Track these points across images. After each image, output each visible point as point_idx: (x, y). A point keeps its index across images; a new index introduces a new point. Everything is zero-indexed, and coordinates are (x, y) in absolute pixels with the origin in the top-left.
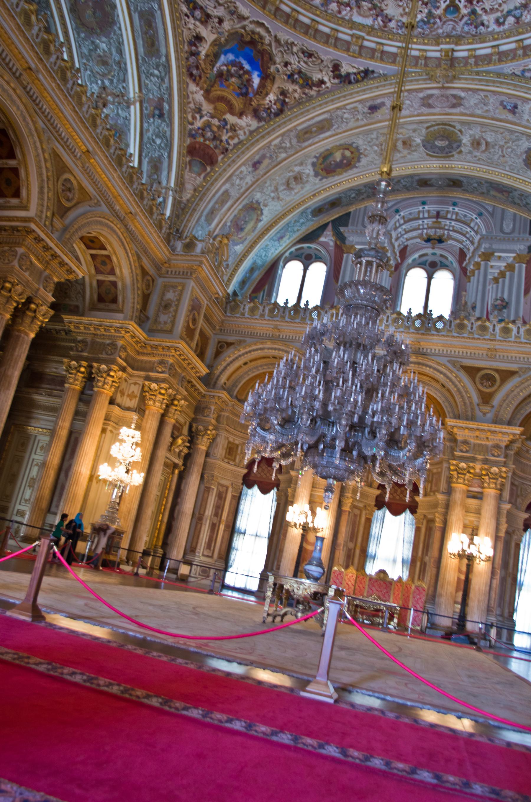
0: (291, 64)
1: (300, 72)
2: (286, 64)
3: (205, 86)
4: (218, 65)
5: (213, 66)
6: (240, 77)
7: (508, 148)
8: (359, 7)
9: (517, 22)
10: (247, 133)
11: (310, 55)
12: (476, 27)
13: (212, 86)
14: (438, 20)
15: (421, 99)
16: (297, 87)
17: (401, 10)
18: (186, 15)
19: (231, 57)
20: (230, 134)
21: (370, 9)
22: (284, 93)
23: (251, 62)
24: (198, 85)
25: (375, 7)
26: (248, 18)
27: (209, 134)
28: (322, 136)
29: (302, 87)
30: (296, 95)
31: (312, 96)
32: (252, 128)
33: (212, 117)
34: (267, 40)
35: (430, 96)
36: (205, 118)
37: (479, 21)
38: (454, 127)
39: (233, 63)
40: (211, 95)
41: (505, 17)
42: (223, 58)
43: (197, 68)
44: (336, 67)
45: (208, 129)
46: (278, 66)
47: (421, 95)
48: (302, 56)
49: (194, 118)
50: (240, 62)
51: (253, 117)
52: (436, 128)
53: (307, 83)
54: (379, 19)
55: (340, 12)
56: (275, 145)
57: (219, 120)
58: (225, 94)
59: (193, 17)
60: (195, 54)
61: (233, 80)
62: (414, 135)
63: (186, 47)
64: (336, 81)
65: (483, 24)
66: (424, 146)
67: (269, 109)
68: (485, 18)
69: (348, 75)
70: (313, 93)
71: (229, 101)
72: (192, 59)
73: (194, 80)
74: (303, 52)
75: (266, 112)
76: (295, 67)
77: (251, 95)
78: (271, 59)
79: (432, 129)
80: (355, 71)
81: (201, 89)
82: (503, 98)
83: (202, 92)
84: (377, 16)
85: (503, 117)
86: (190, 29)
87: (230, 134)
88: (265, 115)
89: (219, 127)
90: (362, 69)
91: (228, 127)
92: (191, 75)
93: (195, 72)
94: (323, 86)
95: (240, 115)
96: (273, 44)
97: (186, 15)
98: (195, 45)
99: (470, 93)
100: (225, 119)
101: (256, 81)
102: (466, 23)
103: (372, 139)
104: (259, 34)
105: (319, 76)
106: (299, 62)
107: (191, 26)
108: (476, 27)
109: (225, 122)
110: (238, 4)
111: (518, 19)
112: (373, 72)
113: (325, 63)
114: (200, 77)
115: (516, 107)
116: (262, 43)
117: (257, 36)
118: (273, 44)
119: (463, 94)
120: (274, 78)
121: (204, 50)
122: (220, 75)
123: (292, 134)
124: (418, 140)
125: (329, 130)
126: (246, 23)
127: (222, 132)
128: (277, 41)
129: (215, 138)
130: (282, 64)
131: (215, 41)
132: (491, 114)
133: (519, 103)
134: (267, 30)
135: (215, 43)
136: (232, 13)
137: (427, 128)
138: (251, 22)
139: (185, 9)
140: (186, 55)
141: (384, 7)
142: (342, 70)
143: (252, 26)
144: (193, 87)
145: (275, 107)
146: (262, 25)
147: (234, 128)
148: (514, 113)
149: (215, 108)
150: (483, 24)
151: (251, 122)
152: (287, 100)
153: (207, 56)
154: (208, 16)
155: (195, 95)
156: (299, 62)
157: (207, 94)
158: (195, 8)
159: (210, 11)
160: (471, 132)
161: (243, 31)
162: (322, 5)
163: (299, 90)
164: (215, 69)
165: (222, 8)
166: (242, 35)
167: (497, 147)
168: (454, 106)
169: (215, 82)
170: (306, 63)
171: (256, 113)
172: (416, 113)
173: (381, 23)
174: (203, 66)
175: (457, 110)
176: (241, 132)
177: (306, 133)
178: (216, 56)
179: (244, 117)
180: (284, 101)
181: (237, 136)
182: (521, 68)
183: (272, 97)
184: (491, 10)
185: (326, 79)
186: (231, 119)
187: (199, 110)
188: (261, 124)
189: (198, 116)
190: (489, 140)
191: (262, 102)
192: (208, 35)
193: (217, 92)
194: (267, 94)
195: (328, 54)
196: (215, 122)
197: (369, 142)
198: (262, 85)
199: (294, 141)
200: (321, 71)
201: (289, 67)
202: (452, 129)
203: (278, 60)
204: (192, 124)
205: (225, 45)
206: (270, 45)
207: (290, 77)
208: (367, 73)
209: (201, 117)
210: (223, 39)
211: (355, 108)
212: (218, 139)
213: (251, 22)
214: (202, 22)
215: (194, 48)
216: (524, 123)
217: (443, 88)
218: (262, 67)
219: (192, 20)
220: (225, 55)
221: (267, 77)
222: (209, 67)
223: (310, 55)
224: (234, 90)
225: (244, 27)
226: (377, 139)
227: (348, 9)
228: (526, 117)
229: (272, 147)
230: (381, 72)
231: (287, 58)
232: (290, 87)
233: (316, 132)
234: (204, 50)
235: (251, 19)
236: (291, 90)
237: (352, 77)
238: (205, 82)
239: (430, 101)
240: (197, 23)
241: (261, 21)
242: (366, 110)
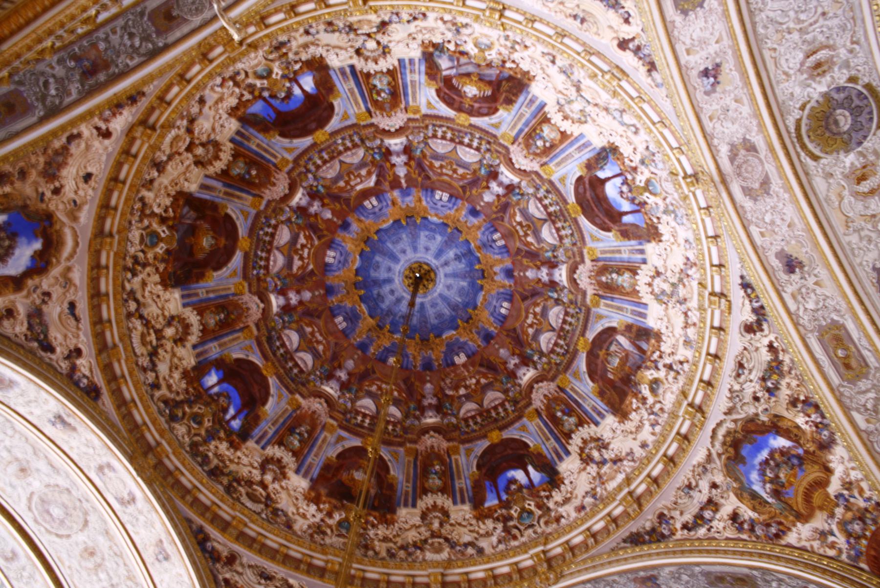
0: (755, 393)
1: (763, 379)
2: (756, 399)
3: (791, 518)
4: (764, 495)
5: (768, 503)
6: (778, 465)
7: (800, 21)
8: (685, 300)
9: (624, 111)
10: (853, 464)
11: (741, 365)
12: (653, 154)
13: (792, 508)
14: (668, 201)
15: (755, 200)
16: (784, 383)
17: (674, 247)
18: (709, 530)
19: (754, 476)
20: (856, 494)
21: (684, 285)
22: (794, 402)
23: (759, 449)
24: (789, 529)
25: (681, 280)
26: (709, 450)
27: (857, 527)
28: (855, 334)
29: (781, 375)
30: (794, 383)
31: (792, 361)
32: (846, 456)
33: (832, 515)
34: (730, 425)
35: (747, 191)
36: (834, 528)
37: (646, 153)
38: (798, 122)
39: (762, 473)
40: (803, 511)
41: (628, 126)
42: (757, 488)
43: (768, 525)
44: (749, 329)
45: (849, 527)
46: (760, 409)
47: (748, 204)
48: (743, 377)
49: (832, 546)
50: (760, 464)
51: (830, 453)
52: (810, 146)
53: (775, 368)
54: (690, 272)
55: (695, 324)
56: (868, 421)
57: (837, 505)
58: (801, 490)
59: (710, 521)
60: (753, 524)
61: (782, 475)
62: (838, 172)
63: (745, 536)
64: (765, 326)
65: (647, 148)
66: (860, 144)
67: (817, 427)
68: (641, 148)
69: (754, 311)
70: (786, 358)
71: (811, 485)
72: (759, 531)
73: (784, 533)
74: (739, 375)
75: (822, 430)
76: (758, 387)
77: (800, 451)
78: (752, 420)
79: (817, 152)
80: (747, 302)
81: (795, 525)
82: (699, 96)
83: (799, 525)
84: (688, 276)
85: (736, 74)
86: (724, 528)
87: (856, 494)
88: (826, 433)
89: (847, 508)
90: (742, 293)
91: (845, 492)
92: (777, 536)
93: (773, 530)
94: (775, 345)
95: (829, 471)
96: (735, 416)
97: (709, 530)
98: (742, 524)
99: (716, 142)
100: (836, 497)
101: (780, 442)
102: (656, 167)
103: (861, 239)
104: (724, 436)
105: (764, 351)
106: (751, 381)
107: (722, 524)
108: (653, 154)
109: (839, 496)
110: (695, 462)
111: (622, 111)
112: (742, 277)
113: (747, 345)
114: (780, 523)
115: (706, 73)
116: (735, 432)
117: (728, 439)
118: (735, 417)
119: (724, 151)
120: (776, 416)
121: (747, 513)
122: (776, 493)
123: (846, 392)
124: (850, 160)
125: (843, 327)
126: (713, 452)
127: (853, 504)
128: (729, 412)
129: (862, 519)
130: (757, 404)
131: (737, 495)
132: (742, 93)
133: (694, 73)
134: (719, 425)
135: (740, 497)
136: (705, 469)
137: (815, 158)
138: (713, 446)
139: (702, 531)
140: (754, 539)
141: (677, 270)
142: (751, 320)
143: (718, 445)
144: (791, 538)
145: (813, 416)
146: (714, 431)
147: (848, 485)
148: (718, 66)
149: (821, 508)
150: (647, 148)
151: (838, 457)
152: (802, 398)
153: (754, 509)
154: (710, 501)
155: (803, 536)
156: (751, 381)
157: (803, 518)
158: (702, 518)
159: (704, 498)
160: (797, 90)
161: (723, 457)
162: (692, 347)
163: (787, 380)
164: (770, 500)
165: (701, 483)
166: (728, 458)
167: (809, 37)
168: (752, 148)
169: (786, 503)
170: (751, 371)
171: (826, 446)
172: (786, 196)
173: (694, 269)
174: (765, 517)
175: (758, 141)
176: (855, 475)
177: (848, 366)
178: (754, 496)
179: (831, 465)
180: (804, 402)
181: (857, 481)
182: (656, 89)
183: (800, 420)
184: (630, 143)
185: (766, 341)
186: (834, 487)
187: (823, 535)
188: (839, 441)
189: (831, 539)
190: (801, 56)
191: (809, 436)
192: (730, 504)
193: (799, 502)
194: (798, 427)
195: (736, 342)
196: (839, 511)
197: (870, 241)
198: (786, 433)
199: (863, 384)
200: (757, 349)
201: (759, 395)
202: (804, 122)
203: (751, 410)
204: (840, 551)
205: (741, 482)
206: (735, 421)
207: (771, 392)
208: (746, 286)
209: (832, 533)
210: (735, 485)
211: (793, 296)
212: (864, 514)
213: (713, 446)
214: (716, 511)
215: (746, 526)
216: (726, 42)
217: (724, 181)
218: (762, 433)
219: (715, 523)
220: (752, 483)
221: (776, 426)
222: (768, 509)
223: (741, 365)
224: (795, 476)
225: (719, 455)
226: (857, 231)
227: (689, 313)
228: (713, 48)
229: (871, 427)
230: (739, 266)
231: (748, 398)
232: (784, 393)
233: (846, 349)
234: (747, 513)
235: (710, 447)
236: (789, 392)
237: (756, 305)
238: (786, 517)
239: (757, 186)
240: (718, 516)
241: (710, 433)
242: (796, 277)
